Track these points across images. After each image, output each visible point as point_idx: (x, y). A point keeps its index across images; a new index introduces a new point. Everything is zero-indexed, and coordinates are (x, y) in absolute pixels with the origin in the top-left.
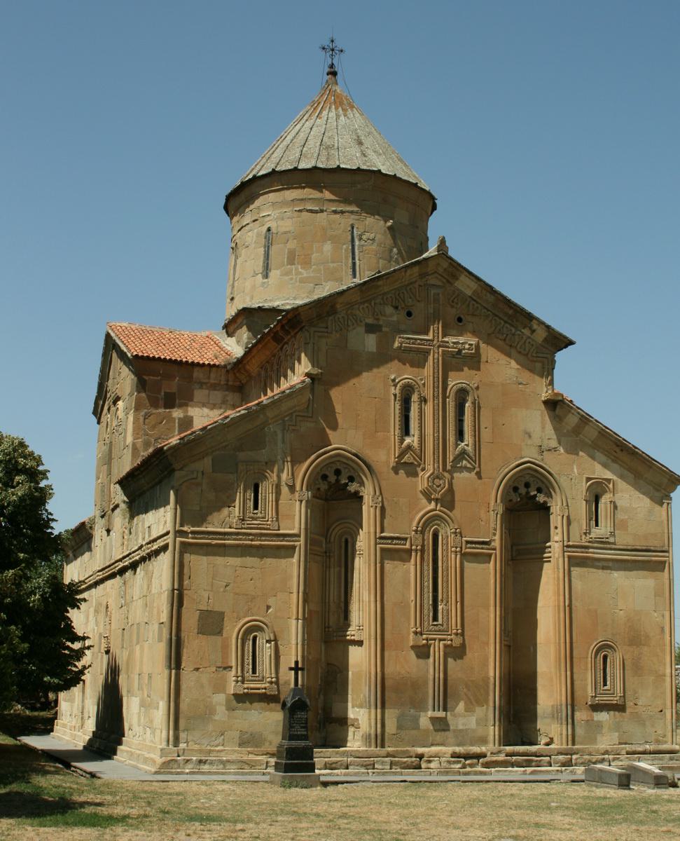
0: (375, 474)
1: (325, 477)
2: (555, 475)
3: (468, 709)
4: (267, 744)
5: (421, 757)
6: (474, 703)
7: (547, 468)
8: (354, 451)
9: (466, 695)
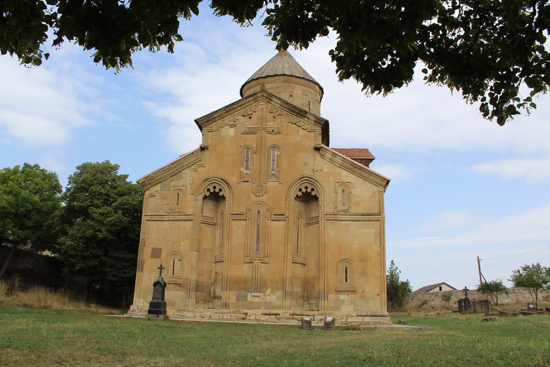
0: (231, 188)
1: (208, 190)
2: (319, 182)
3: (272, 292)
4: (176, 305)
5: (246, 314)
6: (275, 289)
7: (315, 179)
8: (221, 178)
9: (271, 285)
